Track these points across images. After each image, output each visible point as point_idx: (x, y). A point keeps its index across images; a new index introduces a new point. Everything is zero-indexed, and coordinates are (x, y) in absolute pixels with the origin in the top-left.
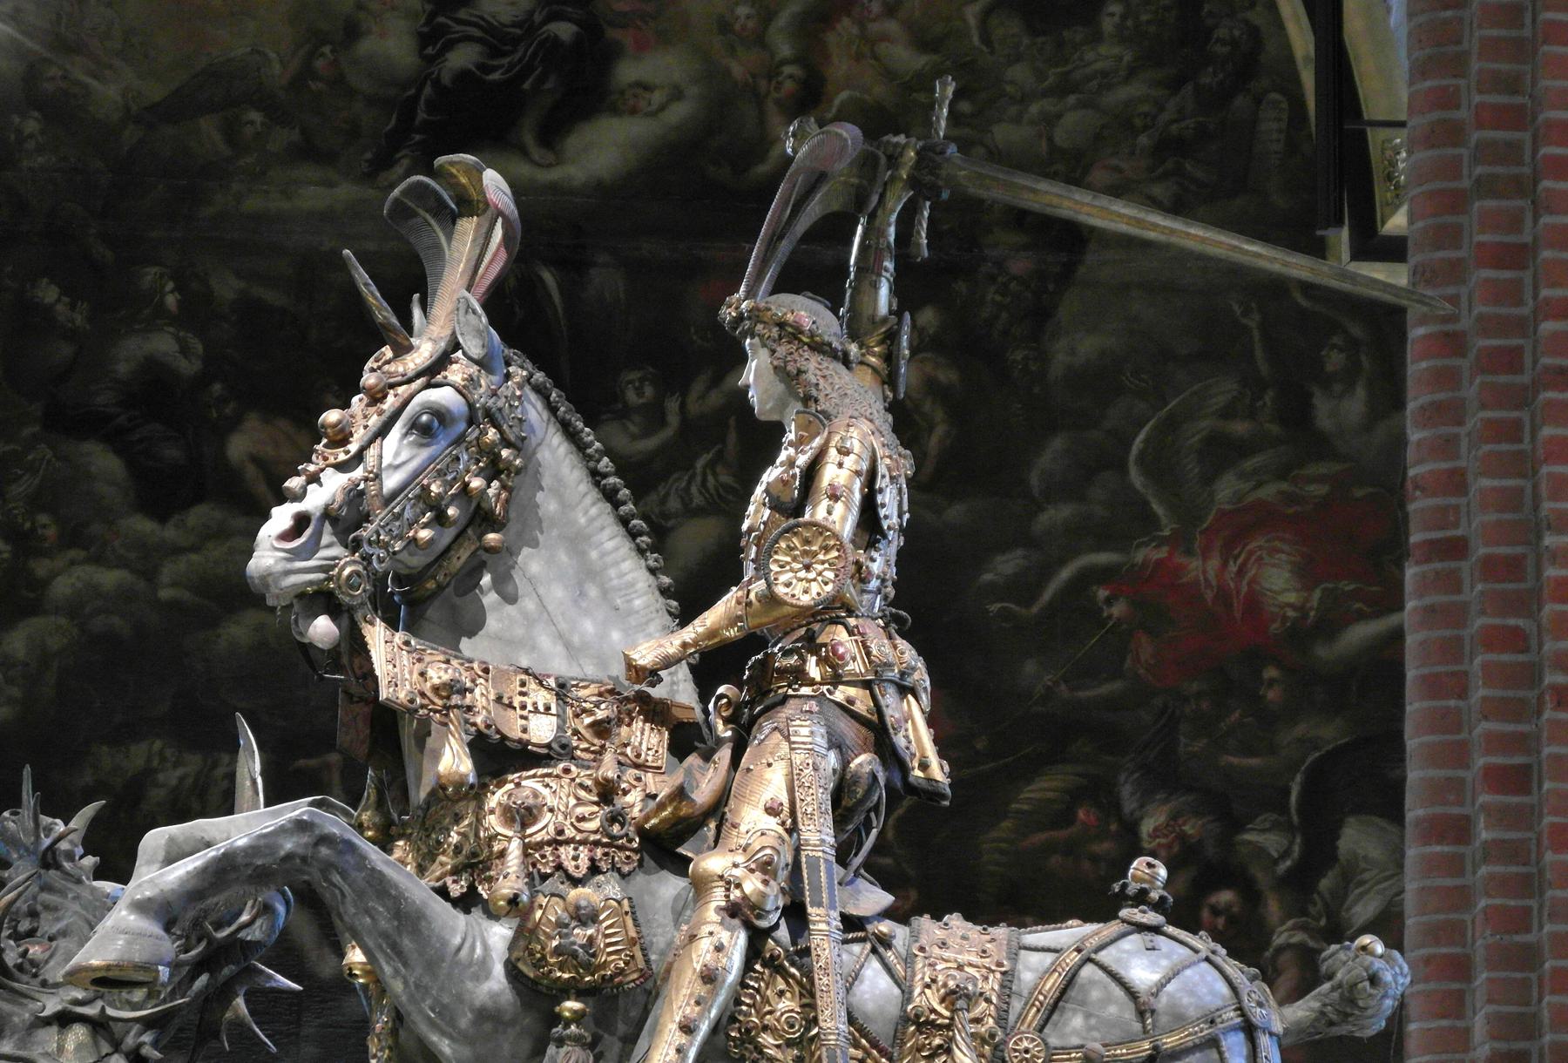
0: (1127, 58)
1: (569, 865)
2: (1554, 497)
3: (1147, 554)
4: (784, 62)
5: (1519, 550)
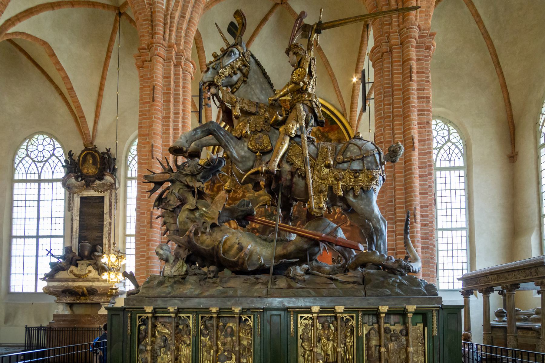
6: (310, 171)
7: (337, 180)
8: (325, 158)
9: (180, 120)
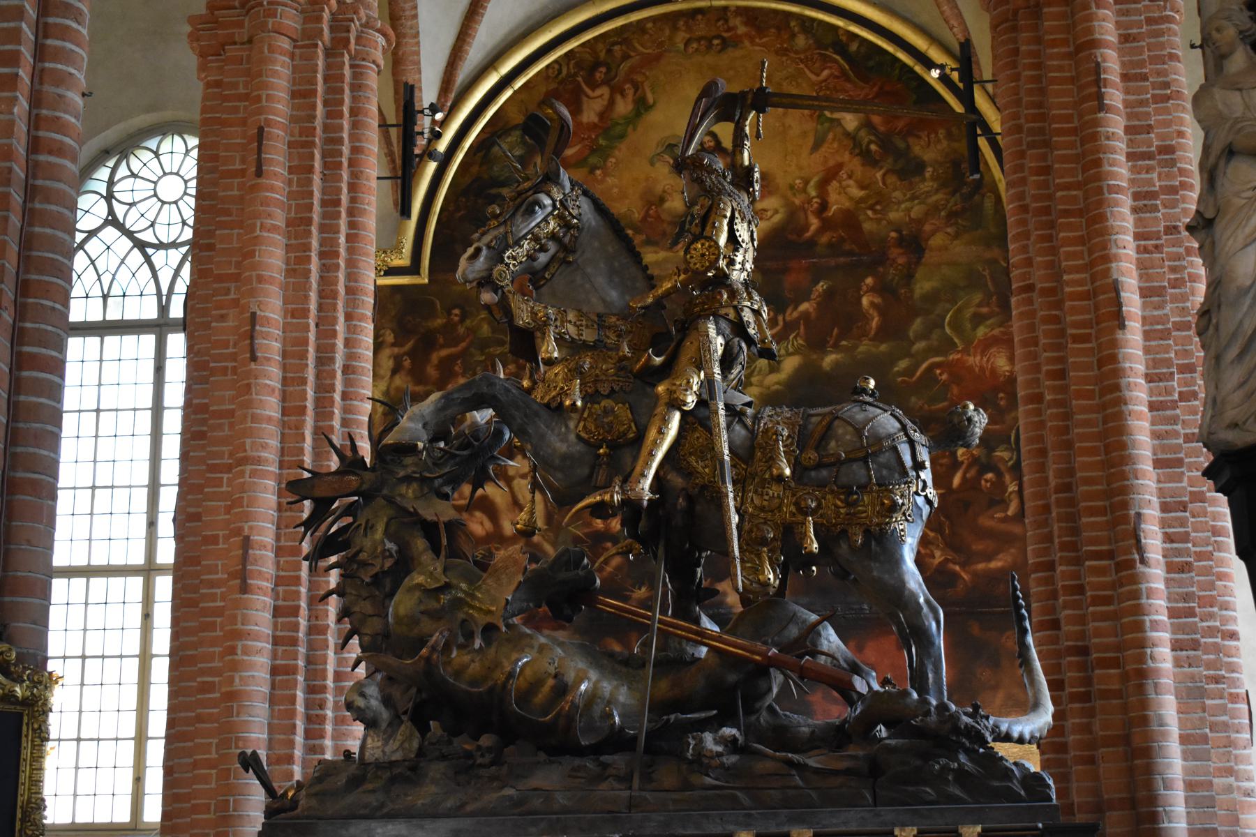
0: (935, 186)
1: (601, 390)
2: (1066, 260)
3: (953, 357)
4: (813, 198)
5: (1055, 284)
6: (731, 495)
7: (805, 512)
8: (772, 460)
9: (343, 223)
